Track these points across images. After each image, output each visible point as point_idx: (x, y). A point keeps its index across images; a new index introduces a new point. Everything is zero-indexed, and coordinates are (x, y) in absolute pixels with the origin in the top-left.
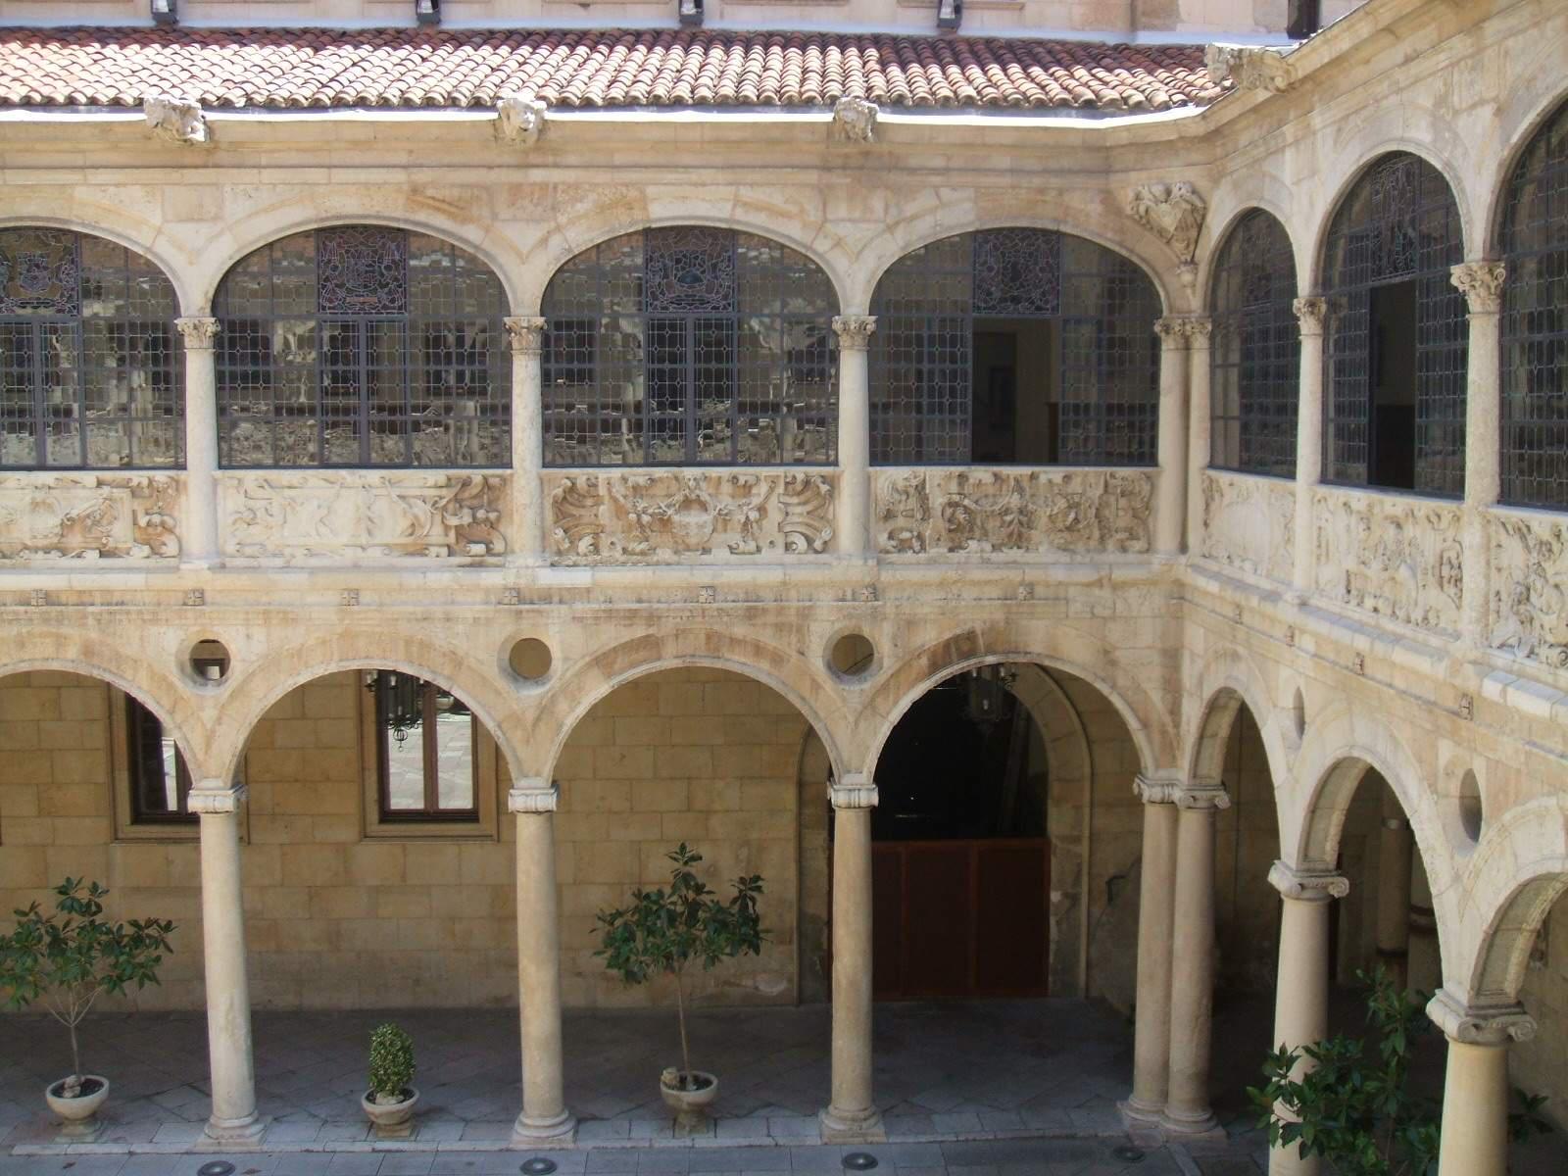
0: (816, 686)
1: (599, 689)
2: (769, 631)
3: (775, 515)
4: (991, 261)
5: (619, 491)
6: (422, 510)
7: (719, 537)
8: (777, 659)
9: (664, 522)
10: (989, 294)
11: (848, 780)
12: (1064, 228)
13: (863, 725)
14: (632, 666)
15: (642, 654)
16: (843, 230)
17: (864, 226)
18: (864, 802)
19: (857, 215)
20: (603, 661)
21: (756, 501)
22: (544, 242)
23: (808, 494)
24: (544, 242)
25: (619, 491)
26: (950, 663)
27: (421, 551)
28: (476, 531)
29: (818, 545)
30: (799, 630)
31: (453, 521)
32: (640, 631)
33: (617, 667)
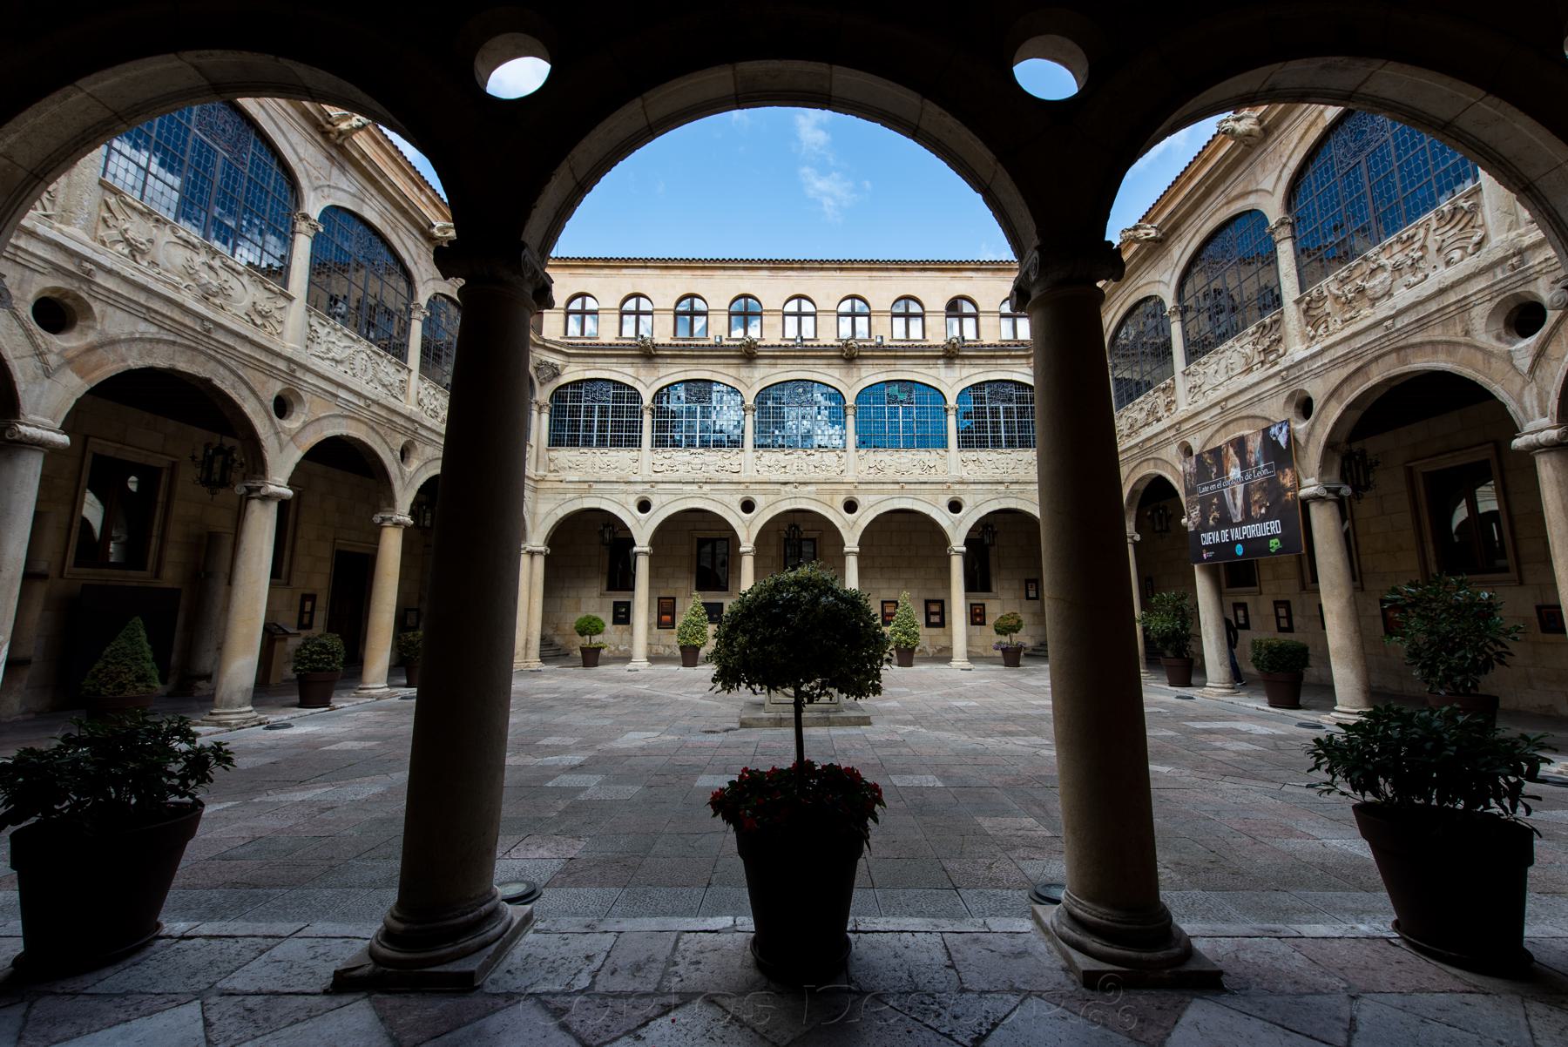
1: (1335, 412)
3: (1433, 247)
5: (1333, 289)
6: (1248, 349)
7: (1399, 281)
9: (1361, 291)
15: (1357, 382)
20: (1334, 394)
21: (1417, 246)
22: (1279, 177)
23: (1458, 217)
24: (1279, 177)
25: (1333, 289)
27: (1249, 370)
28: (1271, 350)
29: (1470, 250)
31: (1260, 348)
32: (1353, 367)
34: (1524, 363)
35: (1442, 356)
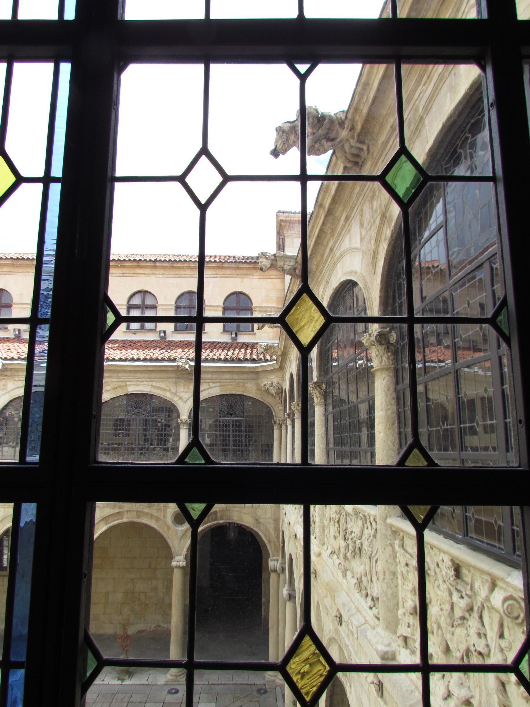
0: (169, 528)
2: (155, 511)
4: (224, 403)
8: (158, 519)
10: (224, 413)
11: (177, 558)
12: (244, 394)
13: (182, 541)
14: (114, 521)
16: (182, 395)
17: (188, 394)
18: (181, 565)
19: (186, 390)
26: (209, 522)
30: (164, 511)
33: (109, 521)
34: (180, 534)
35: (154, 521)
